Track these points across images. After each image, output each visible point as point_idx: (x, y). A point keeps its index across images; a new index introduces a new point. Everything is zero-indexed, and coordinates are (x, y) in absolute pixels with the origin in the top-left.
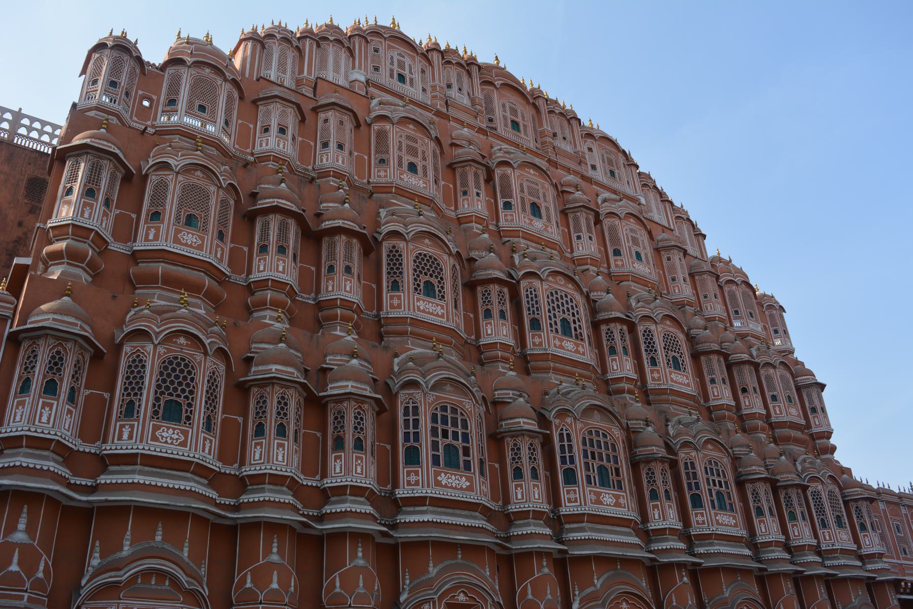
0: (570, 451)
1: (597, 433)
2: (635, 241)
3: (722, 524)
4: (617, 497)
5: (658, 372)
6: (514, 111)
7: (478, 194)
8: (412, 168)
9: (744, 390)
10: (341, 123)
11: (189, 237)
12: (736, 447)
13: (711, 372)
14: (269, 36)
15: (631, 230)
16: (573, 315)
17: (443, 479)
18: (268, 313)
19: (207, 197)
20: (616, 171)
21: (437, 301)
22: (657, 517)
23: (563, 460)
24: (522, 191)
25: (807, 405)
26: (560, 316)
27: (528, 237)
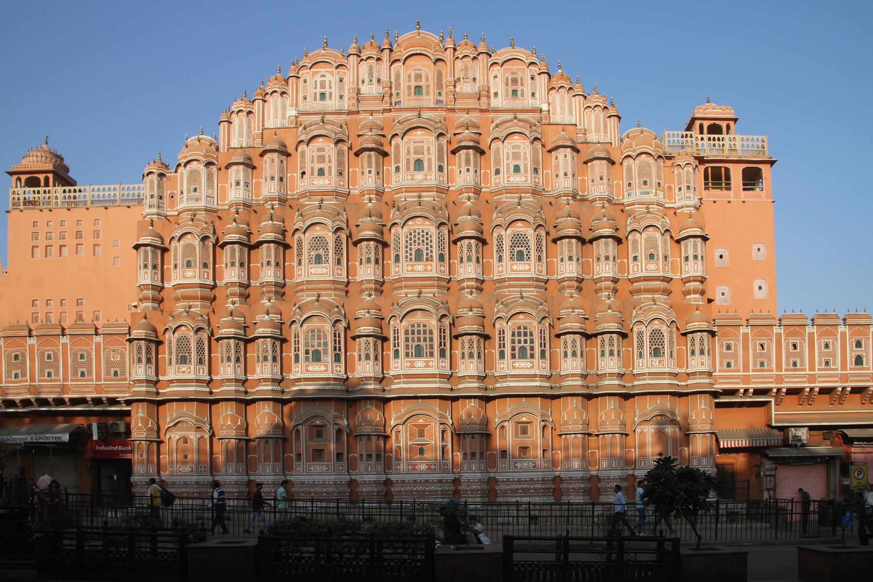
1: (419, 326)
2: (516, 156)
4: (427, 362)
6: (418, 77)
7: (370, 172)
8: (321, 172)
9: (598, 259)
10: (273, 161)
11: (189, 273)
13: (562, 254)
15: (514, 147)
16: (427, 244)
17: (310, 368)
18: (230, 300)
19: (195, 248)
20: (519, 88)
21: (323, 265)
24: (409, 153)
25: (683, 255)
26: (415, 247)
27: (409, 190)
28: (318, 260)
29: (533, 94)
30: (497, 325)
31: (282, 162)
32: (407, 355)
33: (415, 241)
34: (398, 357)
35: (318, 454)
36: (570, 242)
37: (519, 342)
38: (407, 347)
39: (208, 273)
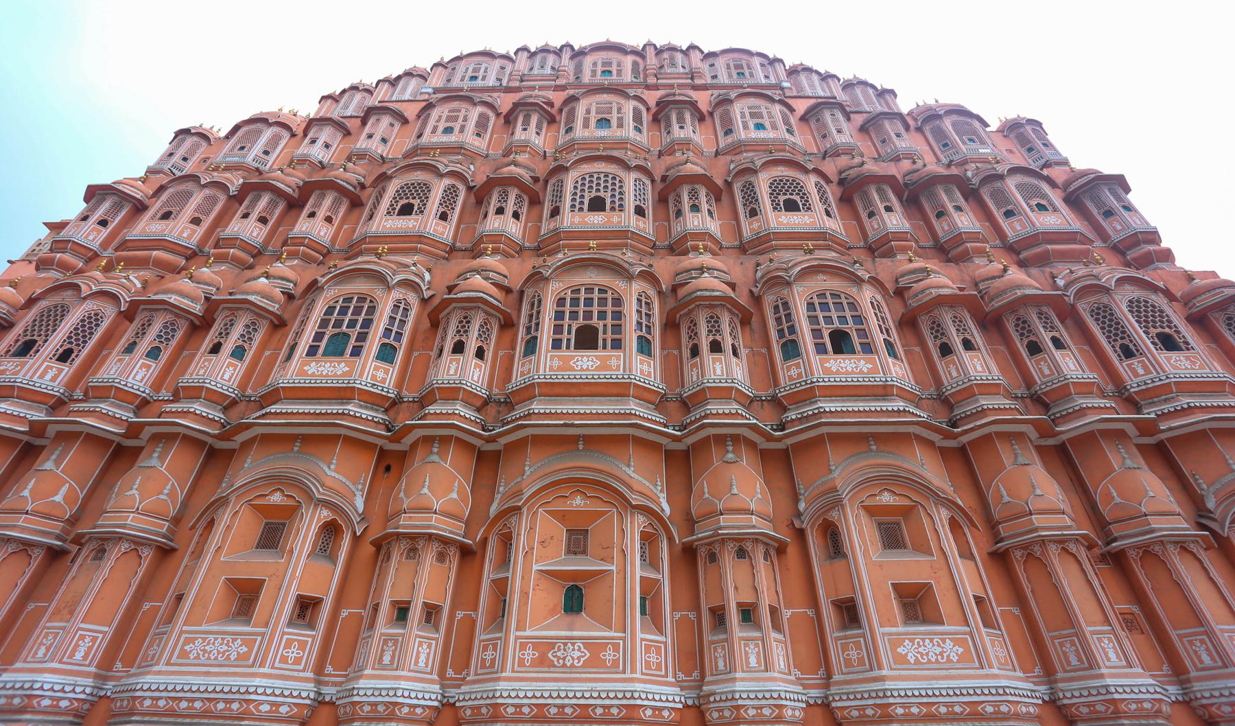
0: (538, 318)
3: (838, 372)
5: (758, 221)
8: (449, 130)
12: (902, 276)
14: (344, 91)
16: (613, 190)
17: (312, 368)
21: (413, 216)
22: (695, 379)
23: (528, 329)
24: (588, 112)
25: (1095, 211)
28: (406, 210)
29: (766, 77)
30: (769, 300)
31: (392, 125)
32: (557, 344)
33: (591, 187)
34: (533, 352)
35: (245, 597)
36: (880, 192)
37: (828, 320)
38: (558, 329)
39: (194, 232)
